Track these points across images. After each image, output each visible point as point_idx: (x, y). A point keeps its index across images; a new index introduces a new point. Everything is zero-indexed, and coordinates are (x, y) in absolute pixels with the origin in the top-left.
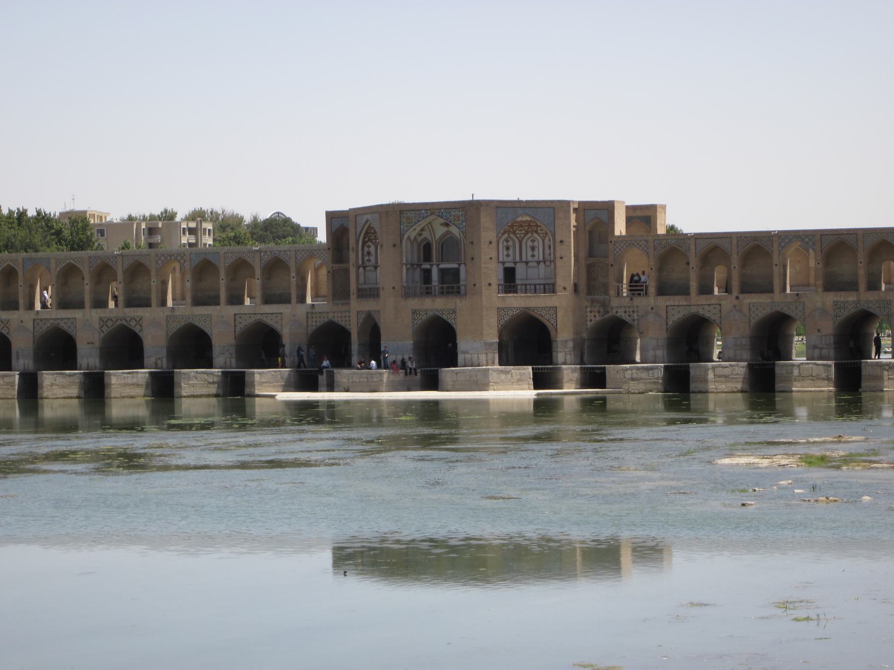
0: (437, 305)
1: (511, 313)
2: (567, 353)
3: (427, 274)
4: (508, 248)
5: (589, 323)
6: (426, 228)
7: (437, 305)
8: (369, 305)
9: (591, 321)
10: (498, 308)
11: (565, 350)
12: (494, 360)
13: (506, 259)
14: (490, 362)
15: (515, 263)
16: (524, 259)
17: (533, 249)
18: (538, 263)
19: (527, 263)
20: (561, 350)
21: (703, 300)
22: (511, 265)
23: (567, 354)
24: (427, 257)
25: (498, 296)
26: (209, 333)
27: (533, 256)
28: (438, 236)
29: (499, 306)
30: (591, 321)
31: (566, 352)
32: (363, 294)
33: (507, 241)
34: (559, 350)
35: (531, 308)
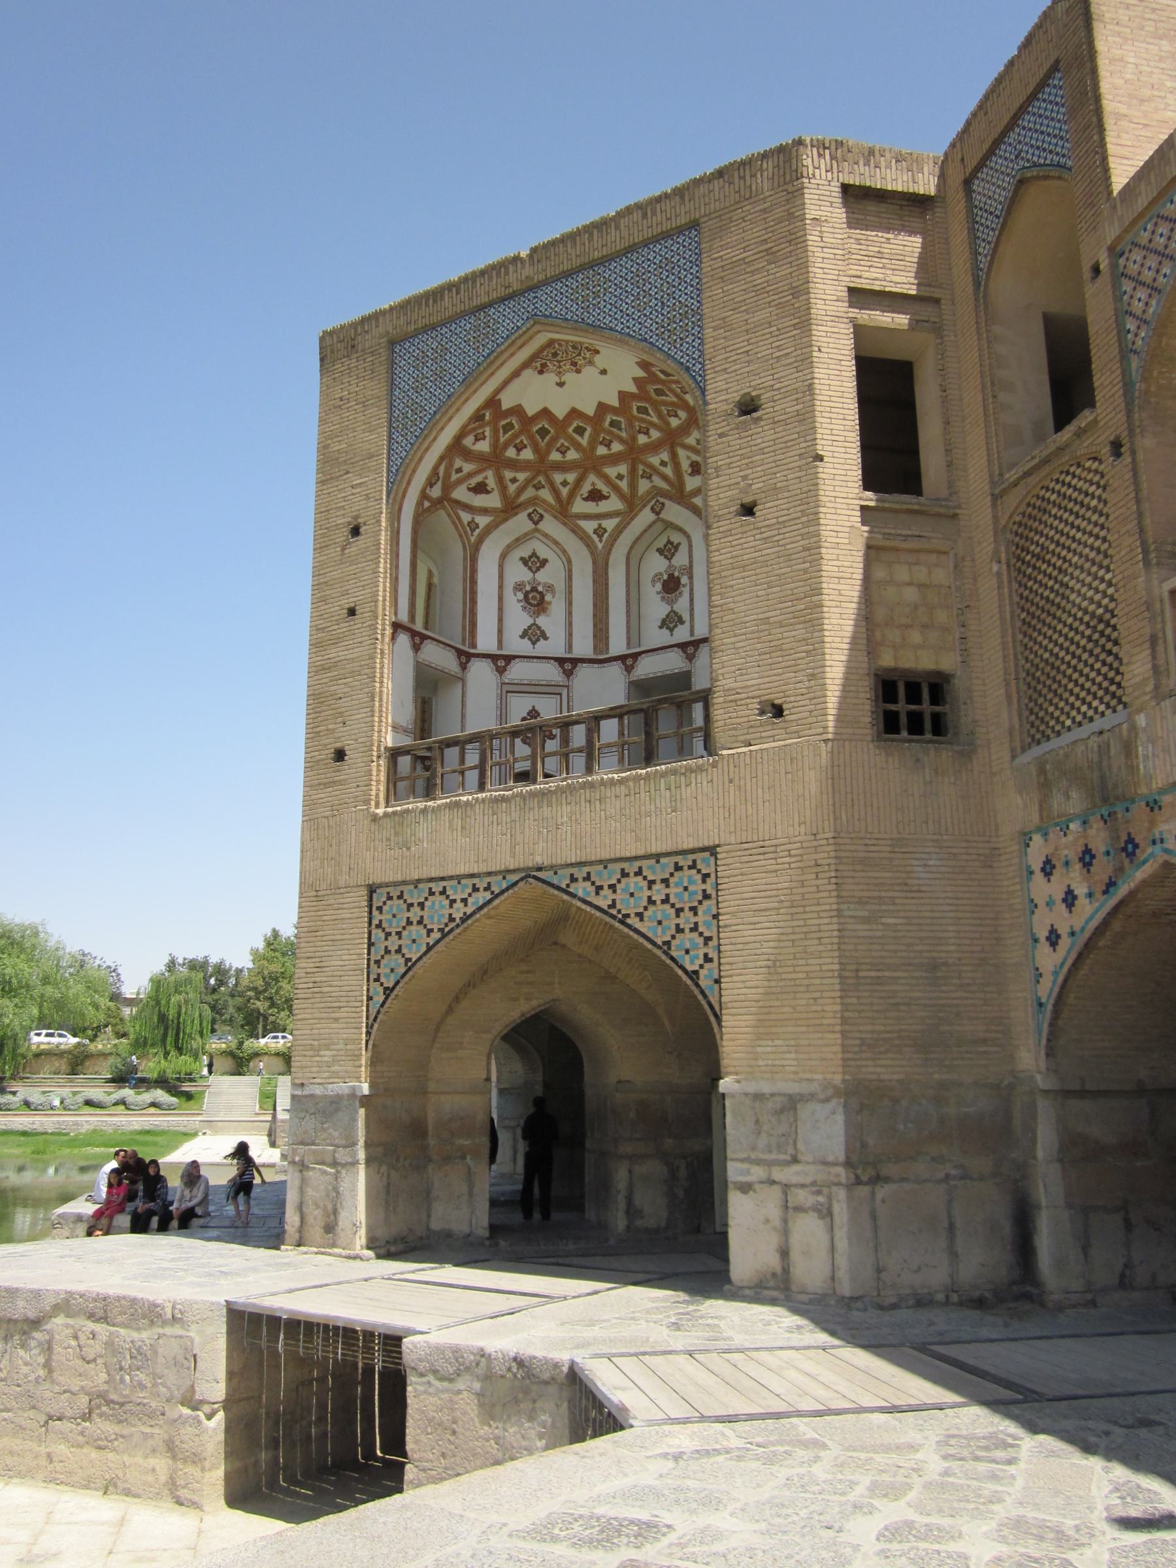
1: (438, 912)
2: (802, 1197)
4: (671, 586)
5: (1050, 960)
9: (1053, 938)
10: (372, 890)
11: (778, 1174)
12: (335, 1212)
14: (315, 1217)
20: (757, 1173)
22: (673, 662)
23: (799, 1209)
25: (375, 818)
29: (377, 878)
30: (1053, 938)
31: (786, 1187)
33: (668, 550)
34: (735, 1171)
35: (554, 869)
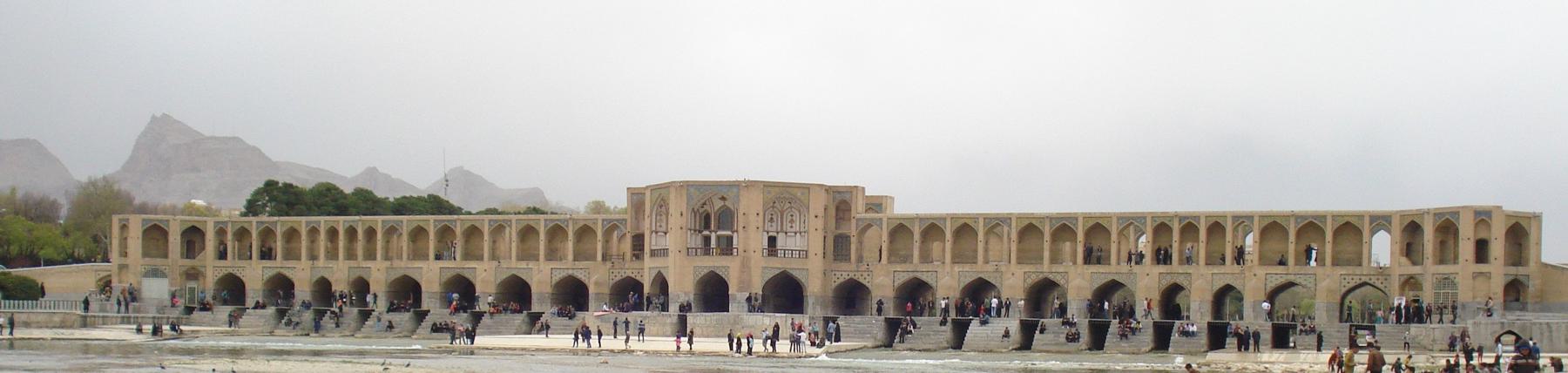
0: (715, 263)
3: (707, 240)
6: (707, 203)
7: (715, 263)
8: (658, 263)
13: (770, 229)
15: (778, 233)
16: (785, 230)
17: (792, 221)
18: (796, 233)
19: (786, 233)
21: (924, 267)
22: (775, 234)
24: (707, 226)
26: (529, 283)
27: (792, 227)
28: (716, 208)
32: (653, 253)
